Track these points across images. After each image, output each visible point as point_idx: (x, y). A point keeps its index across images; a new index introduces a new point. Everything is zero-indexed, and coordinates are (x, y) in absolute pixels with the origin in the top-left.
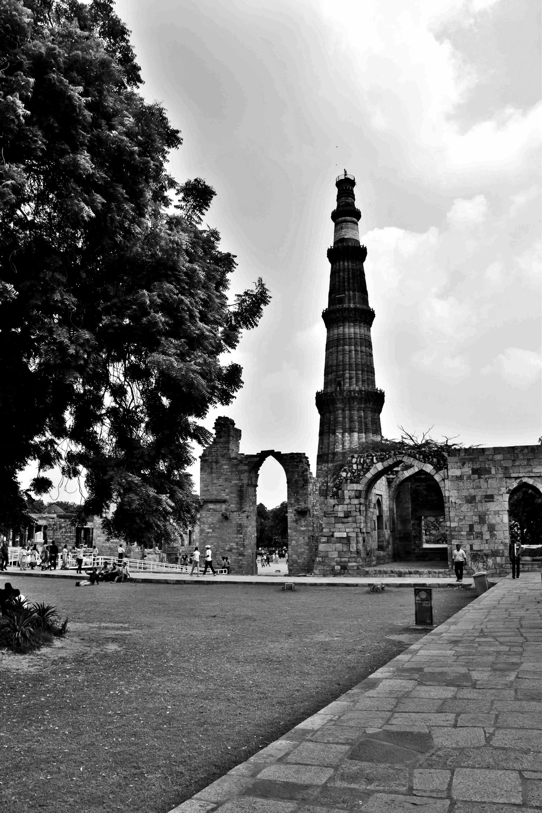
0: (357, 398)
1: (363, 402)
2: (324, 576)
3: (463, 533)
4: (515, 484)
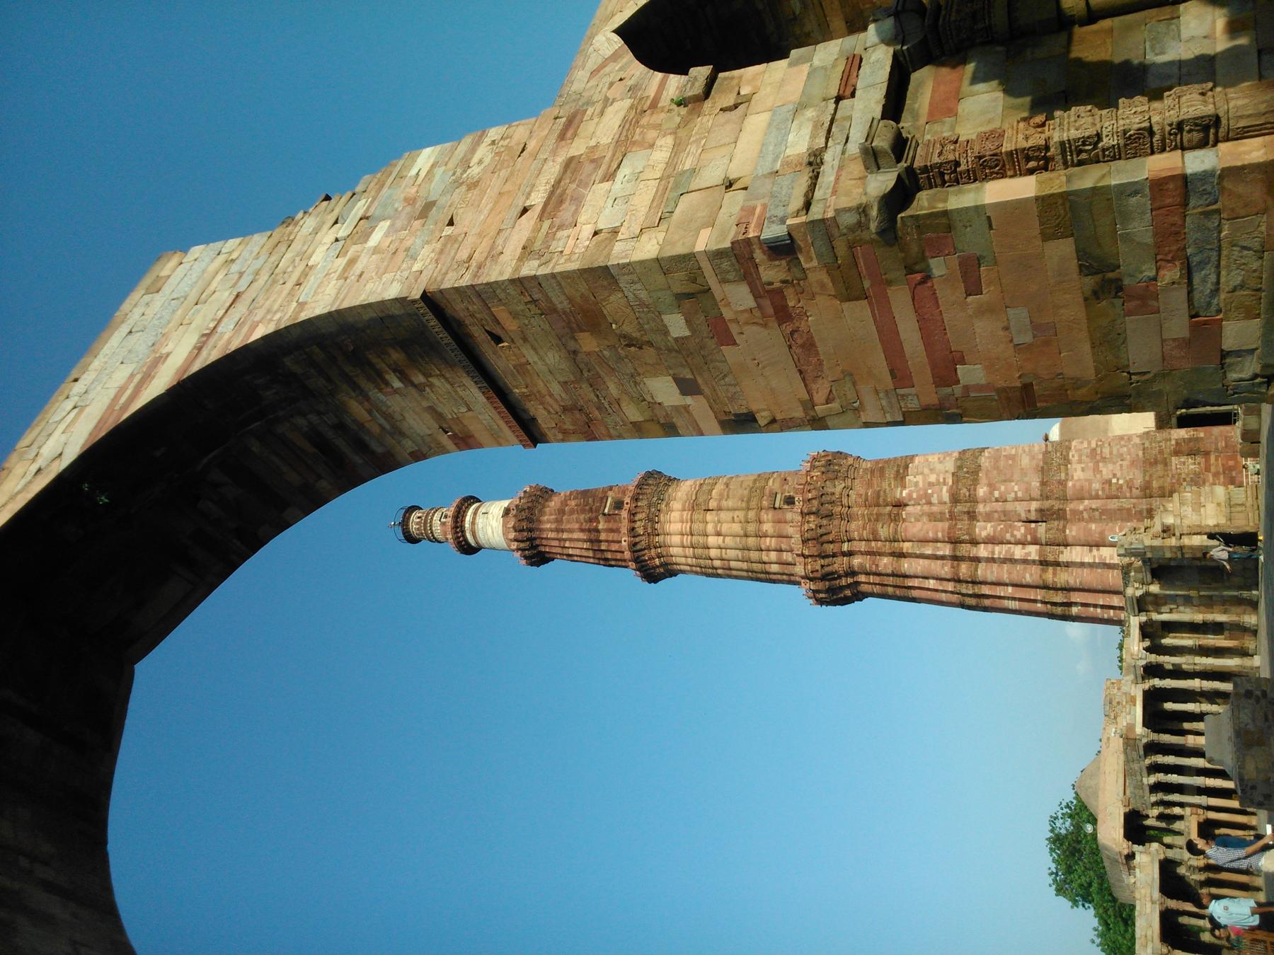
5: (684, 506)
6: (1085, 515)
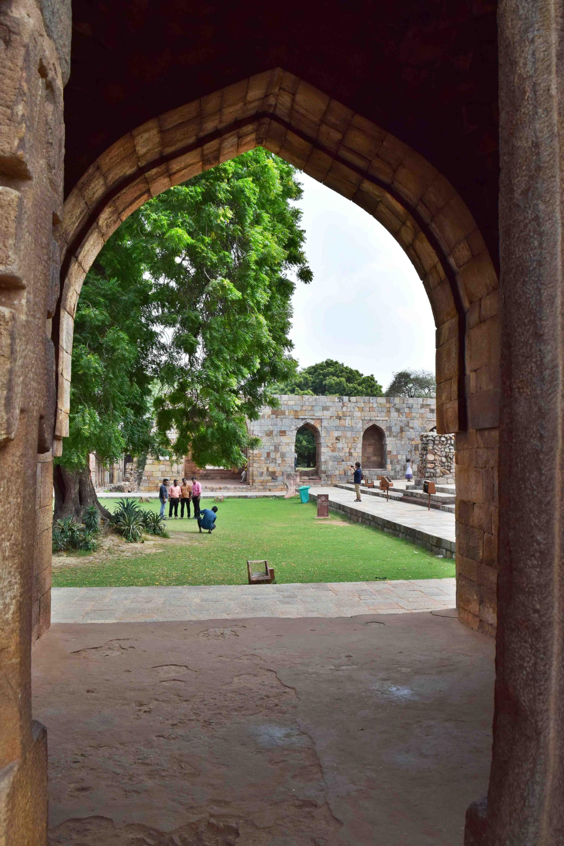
2: (149, 491)
3: (262, 458)
4: (301, 424)
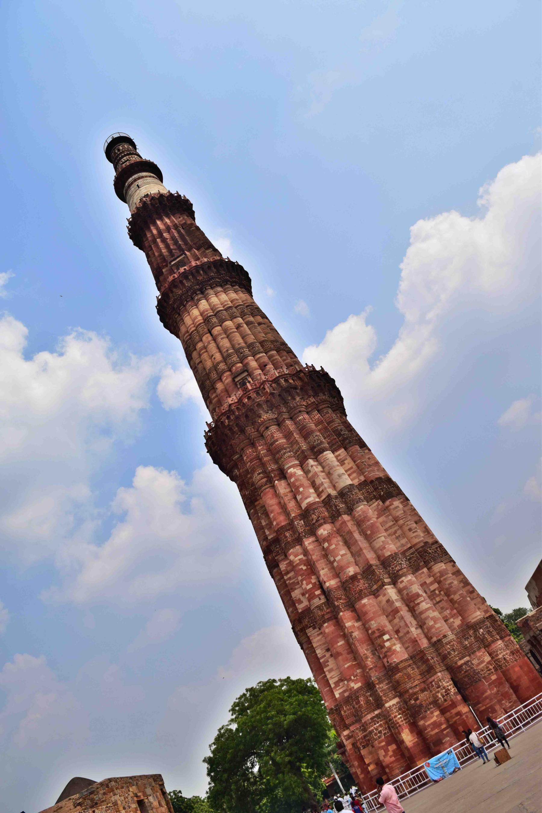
0: (295, 388)
1: (311, 392)
5: (204, 312)
6: (346, 630)
